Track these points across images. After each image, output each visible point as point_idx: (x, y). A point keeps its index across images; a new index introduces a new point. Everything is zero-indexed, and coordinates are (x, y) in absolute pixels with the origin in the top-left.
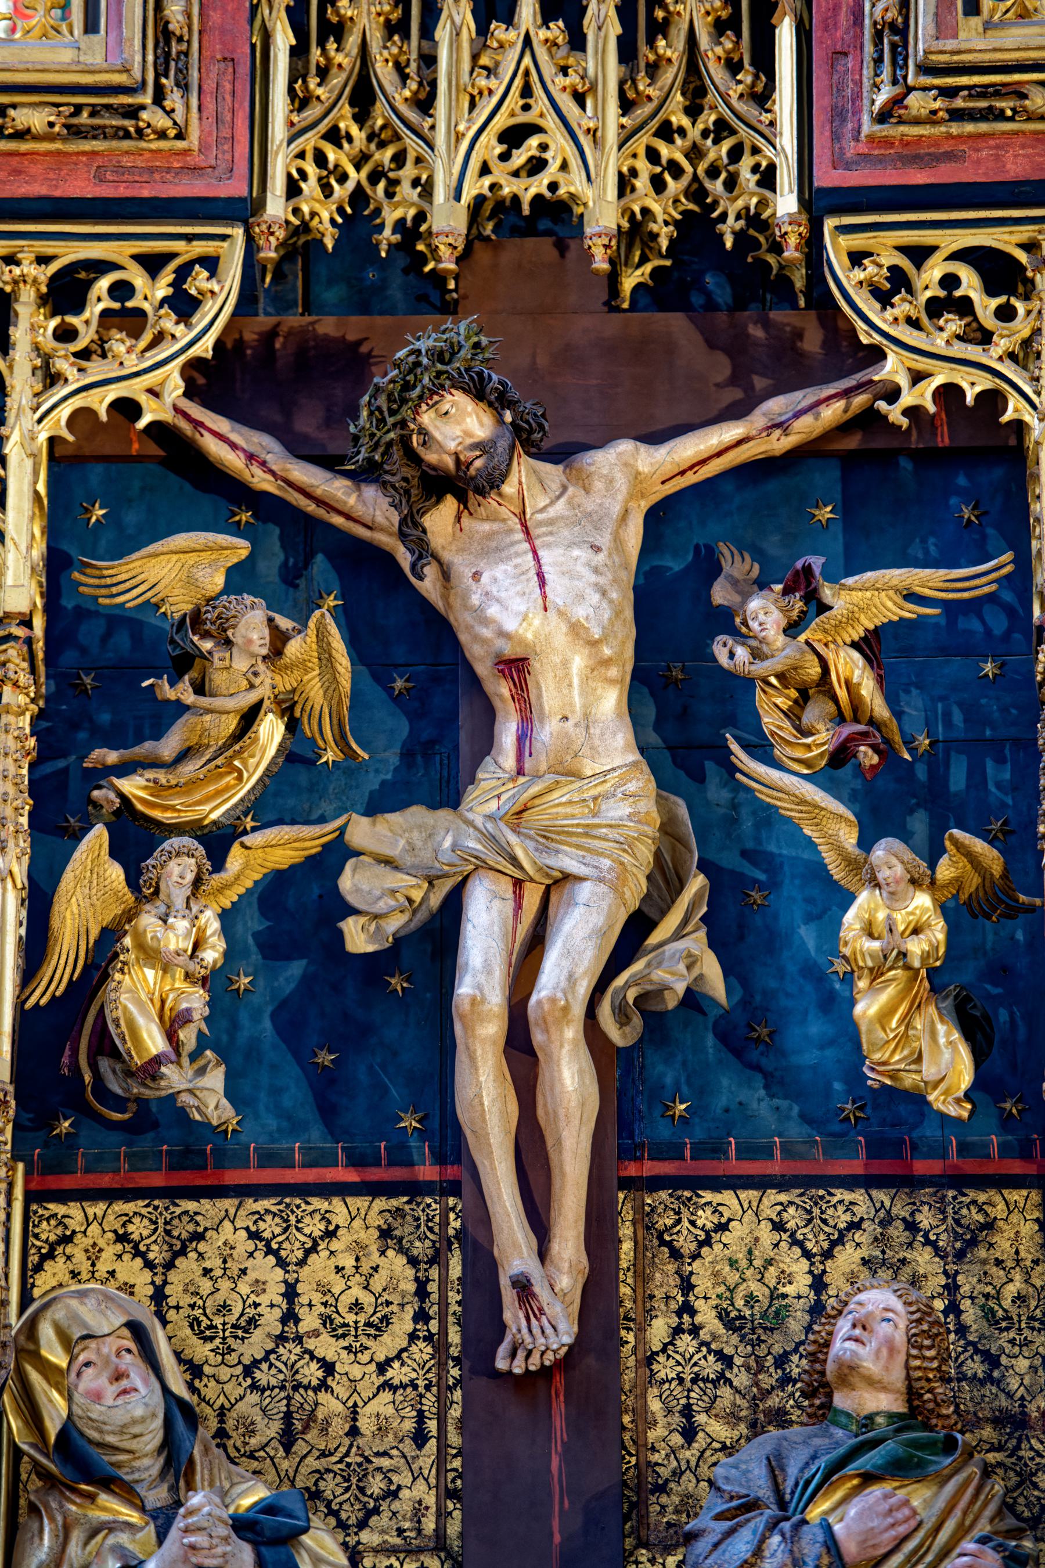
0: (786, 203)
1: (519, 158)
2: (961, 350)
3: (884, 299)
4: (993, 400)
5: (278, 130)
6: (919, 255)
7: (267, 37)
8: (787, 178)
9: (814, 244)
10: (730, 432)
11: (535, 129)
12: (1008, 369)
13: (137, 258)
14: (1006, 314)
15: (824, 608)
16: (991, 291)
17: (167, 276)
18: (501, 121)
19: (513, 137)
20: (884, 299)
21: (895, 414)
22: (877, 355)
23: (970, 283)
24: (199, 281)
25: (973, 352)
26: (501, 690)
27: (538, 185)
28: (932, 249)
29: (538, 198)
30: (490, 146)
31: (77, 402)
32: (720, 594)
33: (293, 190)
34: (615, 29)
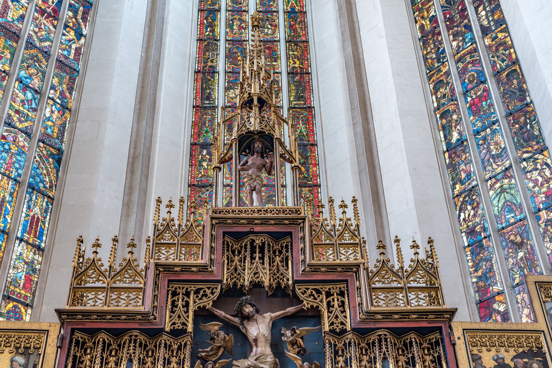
0: (290, 282)
1: (256, 276)
2: (313, 300)
3: (303, 294)
4: (318, 307)
5: (225, 272)
6: (308, 289)
7: (224, 261)
8: (290, 279)
9: (294, 287)
10: (283, 312)
11: (258, 273)
12: (319, 303)
13: (207, 288)
14: (319, 296)
15: (296, 333)
16: (317, 293)
17: (210, 290)
18: (254, 272)
19: (255, 274)
20: (303, 294)
21: (305, 308)
22: (302, 301)
23: (314, 292)
24: (215, 290)
25: (315, 301)
26: (253, 344)
27: (259, 279)
28: (309, 289)
29: (259, 282)
30: (252, 275)
31: (199, 305)
32: (282, 332)
33: (227, 280)
34: (268, 261)
